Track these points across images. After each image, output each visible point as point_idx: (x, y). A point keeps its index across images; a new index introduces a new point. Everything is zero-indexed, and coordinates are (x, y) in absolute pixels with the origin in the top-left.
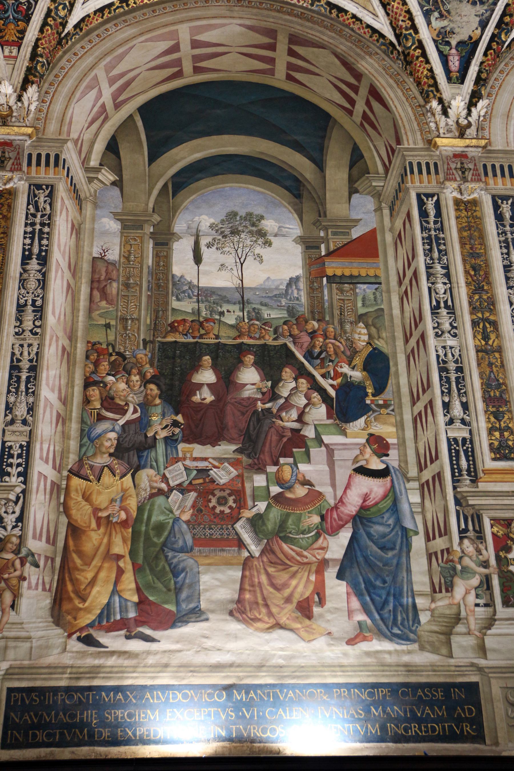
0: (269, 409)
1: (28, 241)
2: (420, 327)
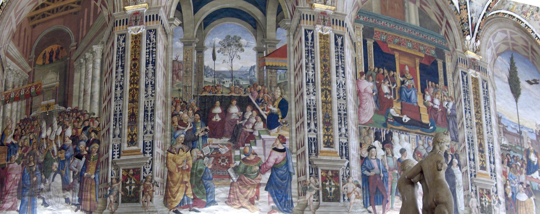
0: (242, 124)
1: (148, 56)
2: (301, 90)
